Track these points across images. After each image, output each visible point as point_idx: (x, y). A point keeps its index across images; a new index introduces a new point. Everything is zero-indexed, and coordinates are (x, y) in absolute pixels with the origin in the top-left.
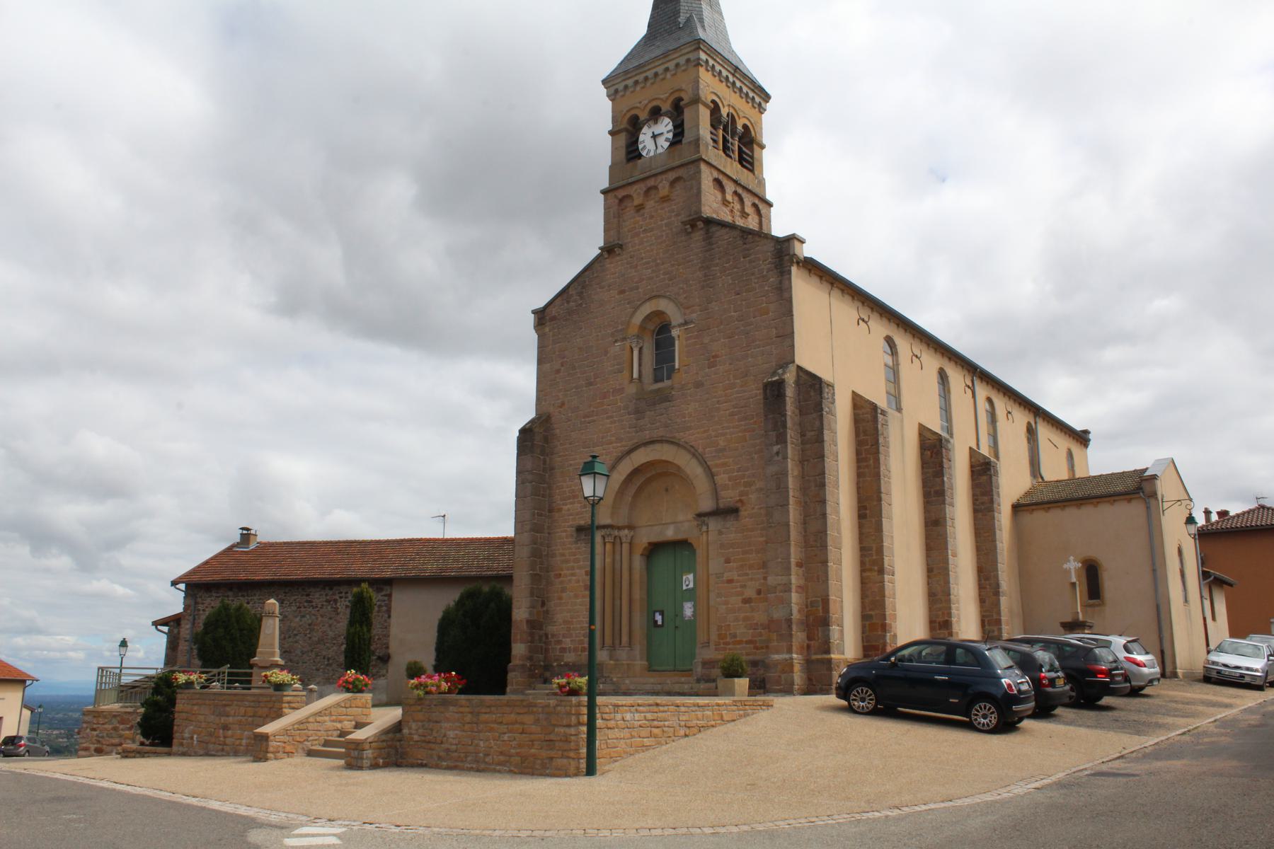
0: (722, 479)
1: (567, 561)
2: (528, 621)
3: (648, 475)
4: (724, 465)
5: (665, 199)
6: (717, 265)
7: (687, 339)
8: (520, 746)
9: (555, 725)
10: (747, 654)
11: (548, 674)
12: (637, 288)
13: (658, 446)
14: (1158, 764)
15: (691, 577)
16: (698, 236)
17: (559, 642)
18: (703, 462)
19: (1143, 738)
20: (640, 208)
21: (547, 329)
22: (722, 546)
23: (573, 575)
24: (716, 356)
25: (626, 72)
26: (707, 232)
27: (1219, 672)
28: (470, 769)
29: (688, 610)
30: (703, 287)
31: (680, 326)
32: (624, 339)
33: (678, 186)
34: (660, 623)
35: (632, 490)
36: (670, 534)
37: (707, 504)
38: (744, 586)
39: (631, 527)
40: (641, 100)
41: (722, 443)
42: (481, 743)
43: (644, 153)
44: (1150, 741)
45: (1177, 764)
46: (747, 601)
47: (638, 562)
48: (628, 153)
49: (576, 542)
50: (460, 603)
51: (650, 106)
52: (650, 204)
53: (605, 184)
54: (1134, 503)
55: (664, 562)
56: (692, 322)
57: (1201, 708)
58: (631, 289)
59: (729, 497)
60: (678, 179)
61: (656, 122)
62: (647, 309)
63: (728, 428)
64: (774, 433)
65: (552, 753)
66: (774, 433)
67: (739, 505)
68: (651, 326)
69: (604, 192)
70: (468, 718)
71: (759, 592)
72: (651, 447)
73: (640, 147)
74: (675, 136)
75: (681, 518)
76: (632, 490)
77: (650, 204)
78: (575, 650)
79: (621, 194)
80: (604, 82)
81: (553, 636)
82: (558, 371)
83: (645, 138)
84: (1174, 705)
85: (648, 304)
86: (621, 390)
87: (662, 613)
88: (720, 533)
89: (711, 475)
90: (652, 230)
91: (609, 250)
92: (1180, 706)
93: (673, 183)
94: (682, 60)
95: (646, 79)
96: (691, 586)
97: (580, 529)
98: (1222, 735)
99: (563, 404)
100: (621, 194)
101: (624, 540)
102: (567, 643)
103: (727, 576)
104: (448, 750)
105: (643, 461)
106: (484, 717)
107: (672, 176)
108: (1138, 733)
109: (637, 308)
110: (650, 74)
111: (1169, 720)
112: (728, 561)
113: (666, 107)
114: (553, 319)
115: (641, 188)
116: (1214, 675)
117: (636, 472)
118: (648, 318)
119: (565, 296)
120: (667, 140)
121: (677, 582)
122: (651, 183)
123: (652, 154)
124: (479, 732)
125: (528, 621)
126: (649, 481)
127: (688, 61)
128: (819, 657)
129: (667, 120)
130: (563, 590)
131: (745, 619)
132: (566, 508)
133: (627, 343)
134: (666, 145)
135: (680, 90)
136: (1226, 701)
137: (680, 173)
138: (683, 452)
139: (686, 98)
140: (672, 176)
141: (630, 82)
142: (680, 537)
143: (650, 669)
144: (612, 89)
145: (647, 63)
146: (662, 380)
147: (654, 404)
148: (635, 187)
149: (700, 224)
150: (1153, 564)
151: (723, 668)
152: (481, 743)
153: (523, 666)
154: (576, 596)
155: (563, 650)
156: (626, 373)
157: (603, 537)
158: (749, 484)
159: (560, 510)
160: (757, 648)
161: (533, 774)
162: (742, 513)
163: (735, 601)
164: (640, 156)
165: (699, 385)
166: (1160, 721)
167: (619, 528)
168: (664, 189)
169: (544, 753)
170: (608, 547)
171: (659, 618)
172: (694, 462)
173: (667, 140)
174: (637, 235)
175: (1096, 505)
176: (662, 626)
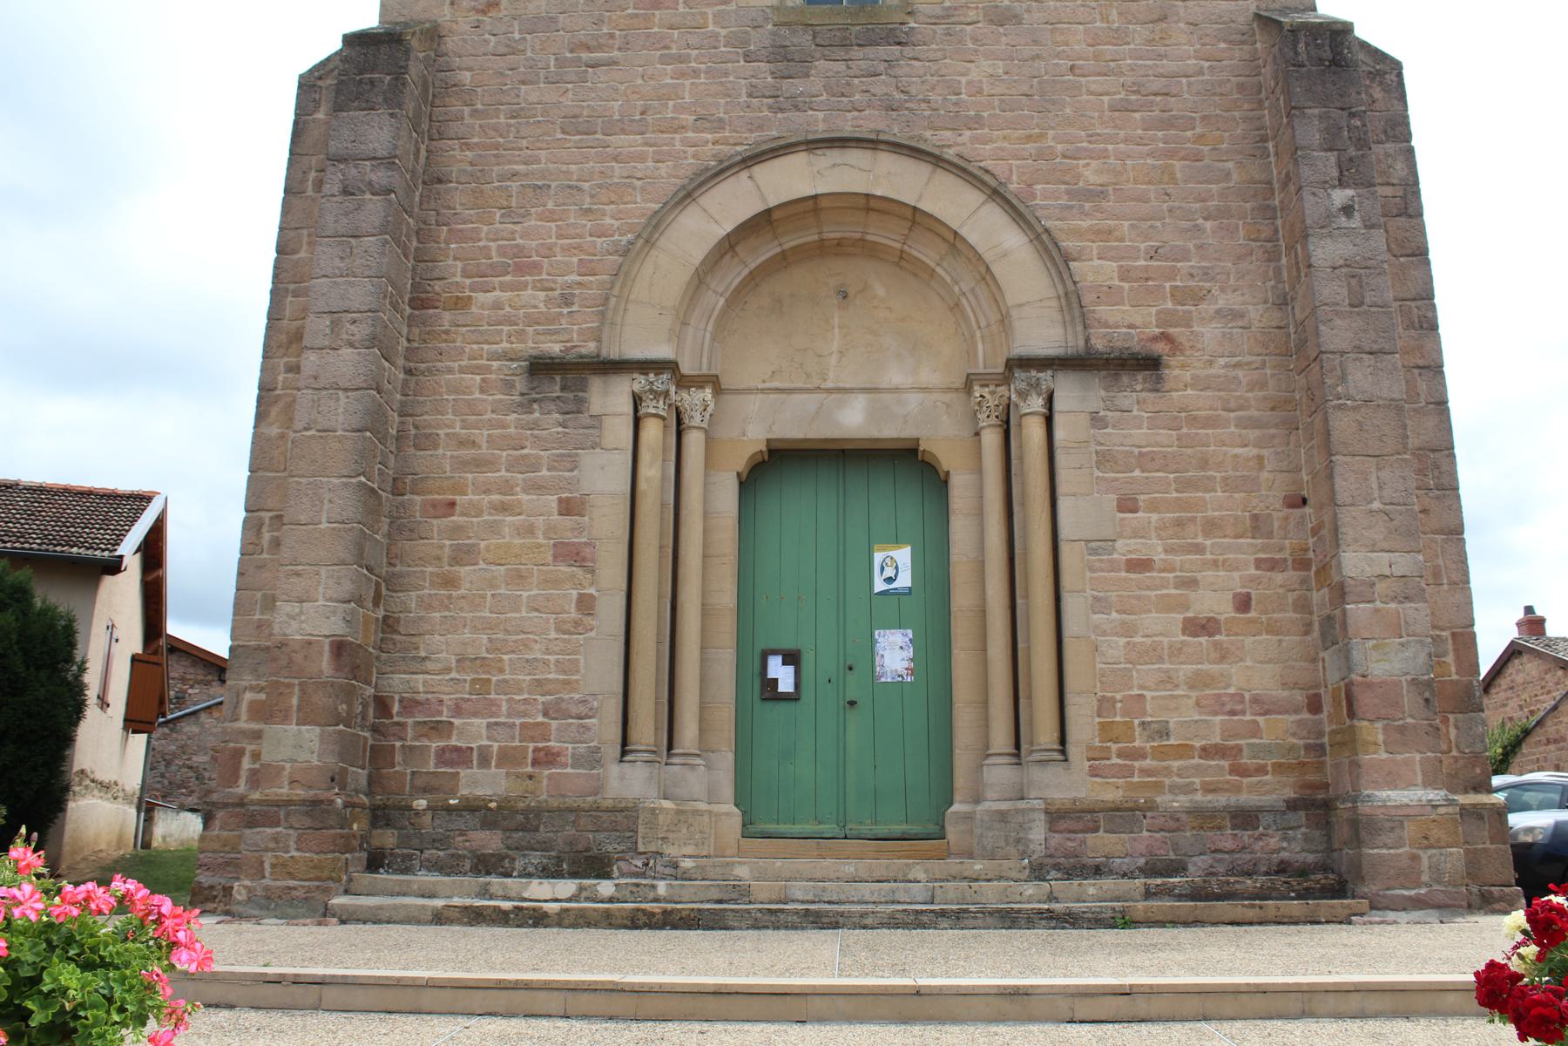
0: (1094, 270)
1: (479, 464)
2: (340, 648)
3: (790, 242)
4: (1105, 234)
10: (1209, 789)
11: (387, 838)
13: (855, 156)
15: (903, 555)
17: (439, 728)
18: (1017, 213)
23: (504, 508)
34: (786, 684)
35: (733, 274)
36: (852, 420)
37: (1042, 334)
38: (1192, 583)
41: (1091, 174)
46: (1202, 627)
47: (716, 497)
49: (526, 405)
55: (801, 508)
59: (1125, 321)
63: (1109, 139)
64: (1332, 157)
66: (1332, 157)
67: (1160, 348)
71: (1243, 603)
72: (834, 156)
75: (895, 376)
76: (733, 274)
81: (410, 705)
87: (791, 658)
88: (1096, 420)
89: (1055, 256)
96: (904, 580)
97: (541, 368)
101: (695, 419)
102: (474, 731)
103: (1125, 548)
105: (806, 190)
112: (1127, 505)
117: (763, 222)
125: (340, 648)
126: (784, 260)
130: (463, 555)
131: (1196, 682)
132: (481, 297)
138: (946, 182)
142: (890, 431)
143: (749, 830)
153: (314, 806)
154: (519, 578)
155: (460, 756)
157: (637, 400)
158: (1198, 297)
159: (461, 303)
160: (1235, 770)
162: (1174, 372)
163: (1162, 626)
170: (652, 432)
171: (783, 676)
176: (786, 697)
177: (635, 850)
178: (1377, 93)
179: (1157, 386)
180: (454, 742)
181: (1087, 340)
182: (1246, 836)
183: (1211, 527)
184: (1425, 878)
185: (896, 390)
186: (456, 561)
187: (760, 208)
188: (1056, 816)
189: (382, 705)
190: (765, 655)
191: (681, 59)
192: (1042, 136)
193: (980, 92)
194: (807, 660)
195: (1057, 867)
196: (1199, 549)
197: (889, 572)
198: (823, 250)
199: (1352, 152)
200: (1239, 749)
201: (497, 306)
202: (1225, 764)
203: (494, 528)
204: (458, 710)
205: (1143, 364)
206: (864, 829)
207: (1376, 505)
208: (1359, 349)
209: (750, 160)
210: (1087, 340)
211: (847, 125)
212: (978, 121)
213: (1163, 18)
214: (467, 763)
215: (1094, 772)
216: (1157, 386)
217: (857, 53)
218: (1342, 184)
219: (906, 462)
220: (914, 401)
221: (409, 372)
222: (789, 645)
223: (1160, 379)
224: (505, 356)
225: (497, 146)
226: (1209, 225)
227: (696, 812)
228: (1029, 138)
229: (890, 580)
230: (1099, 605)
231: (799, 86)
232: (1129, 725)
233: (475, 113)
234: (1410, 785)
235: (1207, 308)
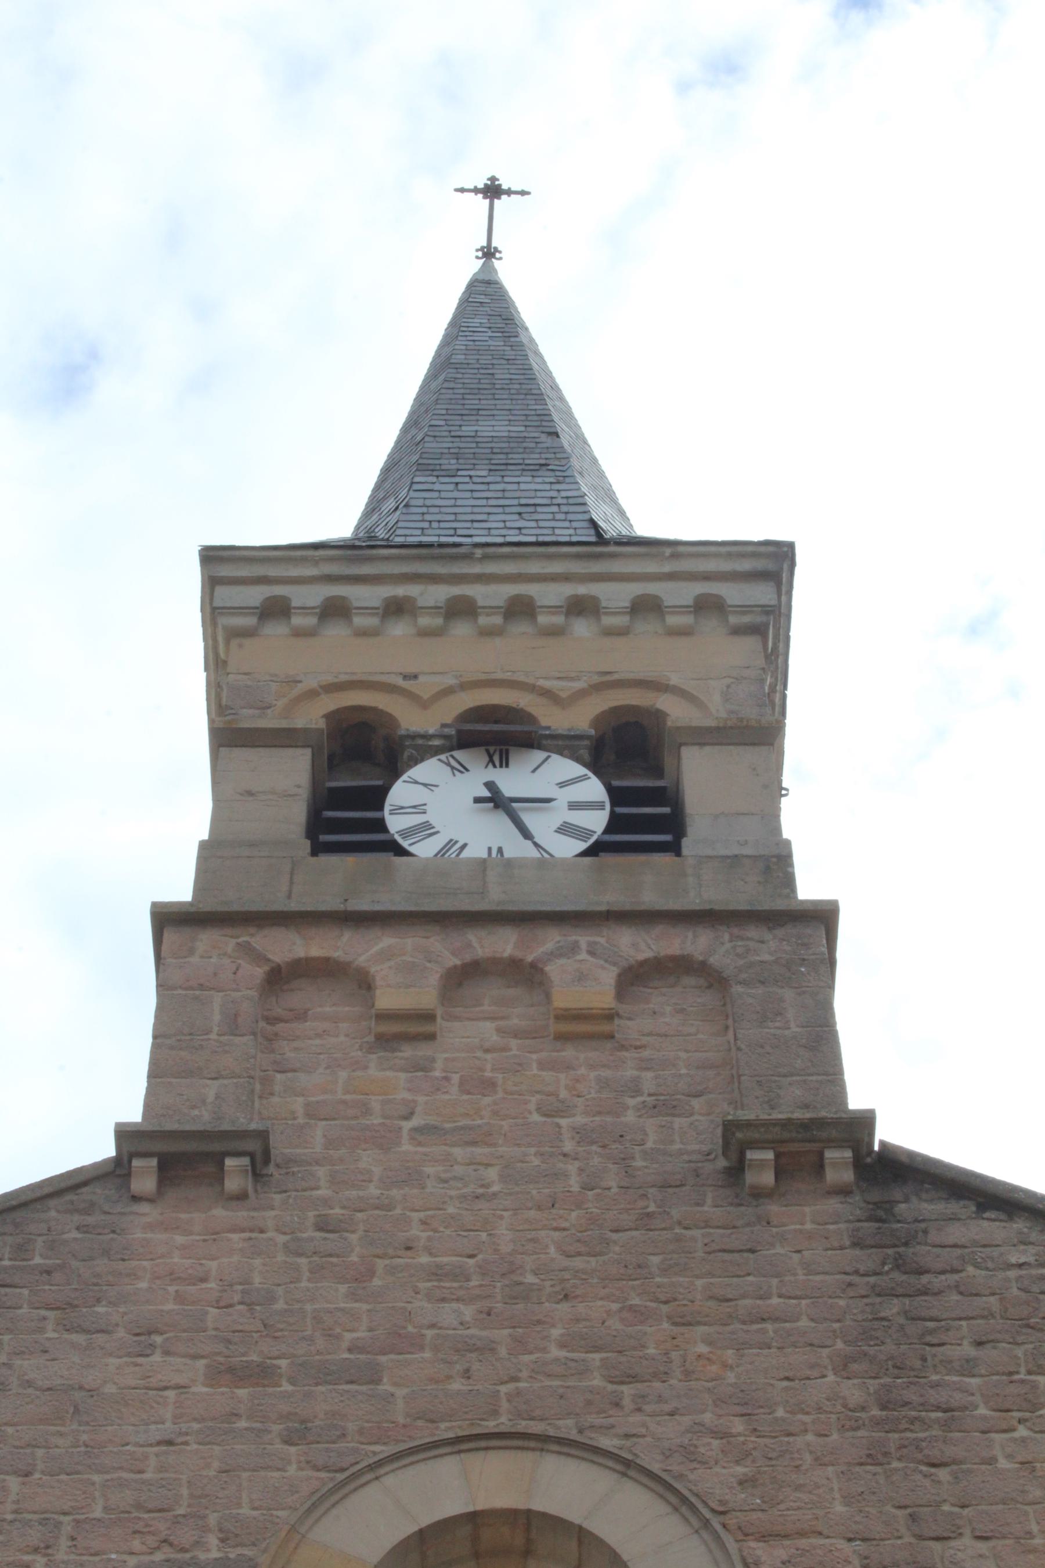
6: (968, 1367)
16: (812, 1231)
20: (404, 1032)
26: (881, 1213)
40: (423, 671)
43: (424, 849)
53: (181, 890)
69: (167, 920)
73: (395, 824)
77: (472, 1034)
79: (286, 946)
85: (447, 1469)
100: (286, 946)
109: (349, 1479)
110: (491, 596)
120: (566, 829)
134: (569, 848)
137: (695, 943)
140: (634, 945)
148: (385, 940)
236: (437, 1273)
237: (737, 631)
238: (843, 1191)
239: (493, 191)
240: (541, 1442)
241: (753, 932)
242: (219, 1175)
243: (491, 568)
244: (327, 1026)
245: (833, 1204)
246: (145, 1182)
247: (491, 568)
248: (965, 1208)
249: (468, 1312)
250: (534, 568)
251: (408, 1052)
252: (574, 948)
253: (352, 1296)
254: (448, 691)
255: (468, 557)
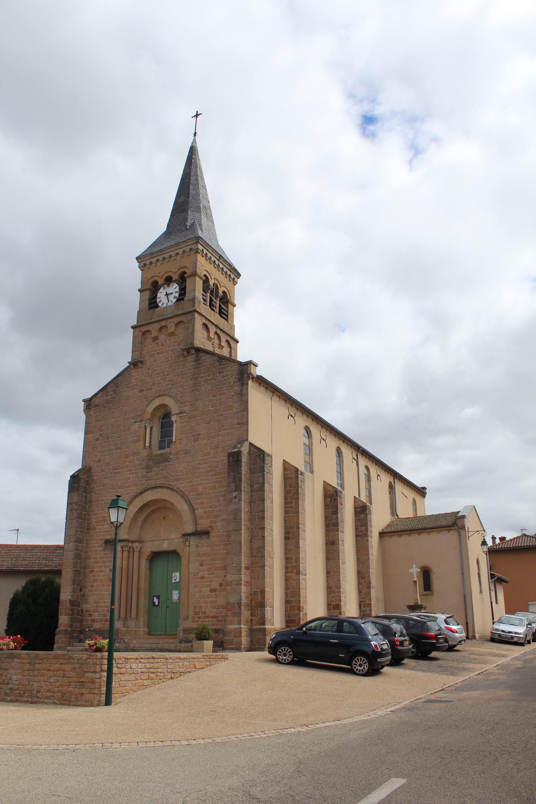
0: (199, 512)
1: (97, 562)
4: (202, 503)
5: (172, 334)
6: (202, 377)
7: (181, 423)
8: (61, 685)
9: (85, 672)
10: (212, 625)
11: (82, 636)
12: (151, 389)
13: (159, 490)
14: (464, 694)
15: (178, 574)
16: (191, 358)
17: (90, 615)
19: (456, 678)
20: (155, 339)
21: (92, 412)
22: (198, 555)
23: (101, 571)
24: (199, 435)
25: (152, 254)
26: (197, 356)
27: (499, 635)
28: (27, 702)
29: (175, 596)
30: (193, 391)
31: (177, 414)
32: (141, 421)
33: (181, 327)
34: (157, 604)
35: (142, 517)
36: (165, 546)
37: (189, 528)
38: (212, 581)
39: (140, 541)
40: (160, 271)
41: (201, 490)
42: (35, 684)
43: (160, 305)
44: (459, 679)
45: (475, 694)
47: (144, 564)
48: (150, 304)
49: (104, 550)
50: (25, 588)
51: (166, 276)
52: (162, 337)
53: (135, 323)
54: (452, 532)
55: (161, 565)
56: (185, 412)
57: (489, 658)
58: (147, 390)
59: (204, 524)
60: (180, 322)
61: (169, 286)
62: (156, 403)
65: (83, 691)
66: (234, 484)
67: (210, 529)
68: (159, 414)
69: (133, 327)
70: (27, 667)
71: (221, 585)
72: (155, 490)
73: (158, 300)
74: (180, 295)
75: (173, 536)
76: (142, 517)
77: (162, 337)
78: (101, 620)
79: (144, 329)
80: (137, 259)
81: (87, 611)
82: (98, 439)
83: (161, 295)
84: (474, 656)
85: (157, 400)
86: (138, 454)
87: (158, 597)
88: (197, 546)
89: (193, 510)
90: (162, 353)
91: (134, 364)
92: (477, 657)
93: (177, 325)
94: (187, 249)
95: (164, 259)
96: (178, 580)
97: (107, 542)
98: (501, 674)
99: (100, 460)
100: (144, 329)
101: (135, 550)
102: (96, 616)
103: (201, 574)
104: (12, 689)
105: (151, 499)
106: (38, 666)
107: (176, 320)
108: (452, 674)
109: (150, 402)
110: (167, 256)
111: (471, 666)
112: (202, 565)
113: (175, 277)
114: (96, 406)
115: (157, 326)
116: (496, 637)
117: (145, 506)
118: (157, 408)
119: (105, 391)
120: (175, 297)
121: (169, 577)
122: (163, 323)
123: (165, 305)
124: (35, 676)
126: (153, 512)
127: (191, 249)
128: (258, 627)
129: (175, 285)
130: (95, 581)
131: (212, 602)
133: (143, 424)
134: (174, 300)
135: (185, 267)
136: (504, 653)
137: (182, 318)
138: (175, 494)
139: (188, 272)
140: (176, 320)
141: (154, 260)
142: (171, 548)
143: (149, 633)
144: (143, 263)
145: (166, 249)
146: (164, 448)
147: (158, 463)
148: (153, 325)
149: (193, 351)
150: (462, 570)
151: (196, 634)
152: (35, 684)
153: (66, 631)
155: (93, 620)
156: (141, 443)
157: (122, 547)
158: (217, 516)
159: (95, 529)
160: (218, 621)
161: (69, 705)
162: (212, 534)
164: (157, 306)
165: (187, 452)
166: (466, 666)
167: (133, 542)
168: (171, 327)
169: (78, 691)
171: (156, 600)
172: (182, 501)
173: (175, 297)
174: (153, 355)
175: (429, 533)
176: (157, 606)
177: (118, 638)
178: (258, 460)
179: (208, 537)
180: (93, 618)
181: (196, 528)
182: (217, 635)
183: (216, 569)
184: (235, 643)
185: (173, 539)
186: (94, 582)
187: (142, 504)
188: (185, 630)
189: (82, 611)
190: (154, 596)
191: (131, 470)
192: (192, 481)
193: (182, 472)
194: (161, 597)
195: (184, 641)
196: (213, 573)
197: (175, 578)
198: (159, 509)
199: (238, 483)
200: (218, 616)
201: (100, 529)
202: (215, 619)
203: (99, 575)
204: (93, 612)
205: (206, 533)
206: (169, 633)
207: (234, 565)
208: (234, 530)
209: (141, 493)
210: (196, 528)
211: (159, 482)
212: (181, 479)
213: (217, 448)
214: (94, 622)
215: (193, 622)
216: (208, 537)
217: (161, 465)
218: (235, 491)
219: (172, 555)
220: (176, 541)
221: (87, 544)
222: (158, 594)
223: (209, 536)
224: (101, 540)
225: (100, 494)
226: (222, 498)
227: (131, 630)
228: (190, 482)
229: (175, 580)
230: (196, 587)
231: (150, 474)
232: (199, 612)
233: (97, 487)
234: (235, 624)
235: (219, 519)
236: (157, 374)
237: (195, 253)
238: (194, 354)
239: (197, 115)
240: (164, 395)
241: (188, 315)
242: (138, 365)
243: (167, 251)
244: (149, 340)
245: (193, 356)
246: (132, 368)
247: (167, 251)
248: (204, 354)
249: (160, 378)
250: (171, 250)
251: (156, 341)
252: (170, 322)
253: (150, 379)
254: (163, 274)
255: (164, 251)
